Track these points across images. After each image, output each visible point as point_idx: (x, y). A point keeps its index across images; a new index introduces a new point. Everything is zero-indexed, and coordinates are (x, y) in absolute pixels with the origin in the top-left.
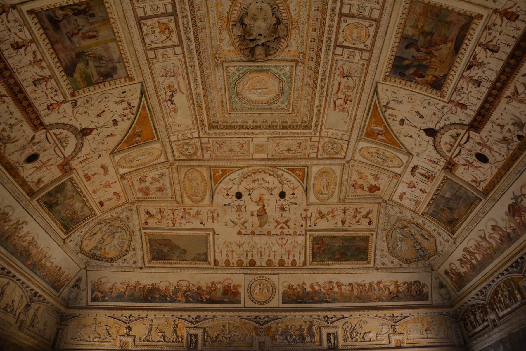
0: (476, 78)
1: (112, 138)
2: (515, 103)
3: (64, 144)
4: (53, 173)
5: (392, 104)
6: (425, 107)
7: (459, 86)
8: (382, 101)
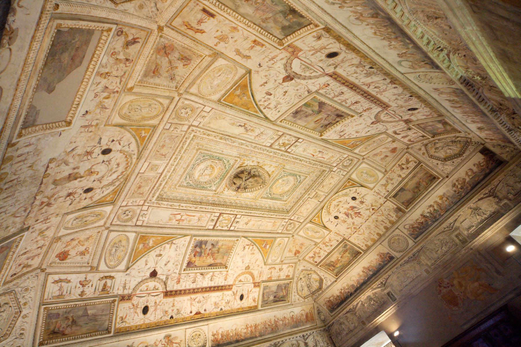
0: (197, 279)
1: (262, 83)
2: (189, 302)
3: (304, 67)
4: (305, 44)
5: (174, 246)
6: (173, 264)
7: (190, 274)
8: (177, 240)
